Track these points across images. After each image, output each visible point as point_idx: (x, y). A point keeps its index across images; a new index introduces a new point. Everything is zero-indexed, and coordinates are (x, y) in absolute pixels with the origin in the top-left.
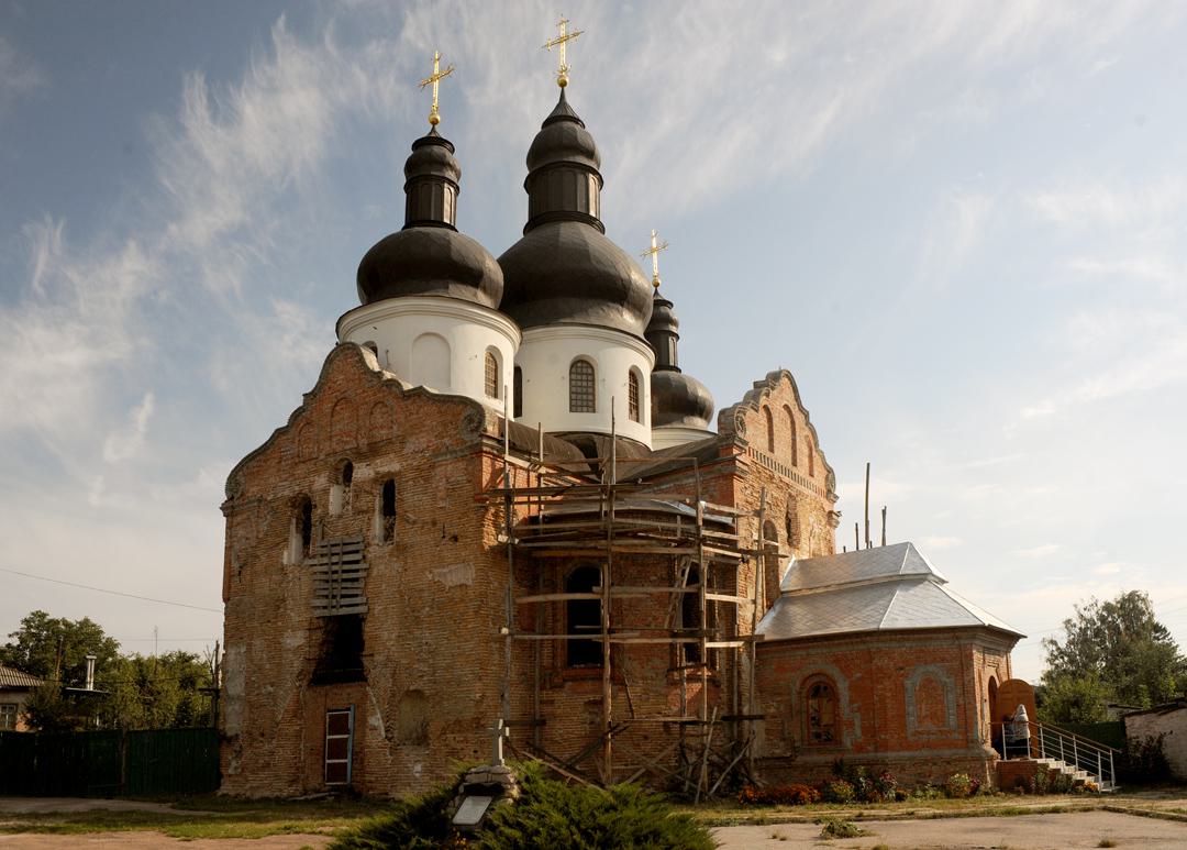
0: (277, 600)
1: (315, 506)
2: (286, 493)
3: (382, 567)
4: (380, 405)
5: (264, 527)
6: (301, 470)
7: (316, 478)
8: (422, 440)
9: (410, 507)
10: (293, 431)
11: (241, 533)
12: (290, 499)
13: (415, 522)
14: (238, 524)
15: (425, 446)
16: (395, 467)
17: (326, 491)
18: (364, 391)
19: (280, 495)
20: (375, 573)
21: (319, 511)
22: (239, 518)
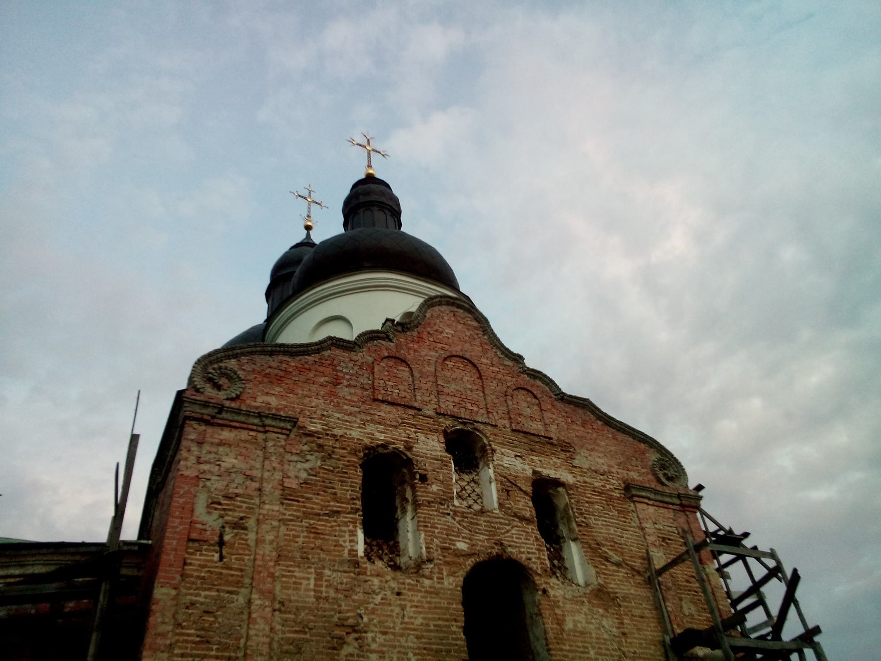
0: (341, 625)
1: (424, 478)
2: (355, 434)
3: (577, 617)
4: (524, 392)
5: (298, 471)
6: (384, 411)
7: (422, 437)
8: (601, 461)
9: (606, 540)
10: (364, 356)
11: (230, 461)
12: (366, 448)
13: (618, 565)
14: (221, 444)
15: (605, 468)
16: (567, 477)
17: (446, 465)
18: (493, 365)
19: (338, 432)
20: (569, 625)
21: (434, 488)
22: (226, 434)
